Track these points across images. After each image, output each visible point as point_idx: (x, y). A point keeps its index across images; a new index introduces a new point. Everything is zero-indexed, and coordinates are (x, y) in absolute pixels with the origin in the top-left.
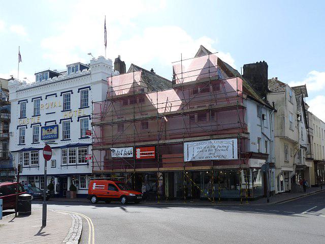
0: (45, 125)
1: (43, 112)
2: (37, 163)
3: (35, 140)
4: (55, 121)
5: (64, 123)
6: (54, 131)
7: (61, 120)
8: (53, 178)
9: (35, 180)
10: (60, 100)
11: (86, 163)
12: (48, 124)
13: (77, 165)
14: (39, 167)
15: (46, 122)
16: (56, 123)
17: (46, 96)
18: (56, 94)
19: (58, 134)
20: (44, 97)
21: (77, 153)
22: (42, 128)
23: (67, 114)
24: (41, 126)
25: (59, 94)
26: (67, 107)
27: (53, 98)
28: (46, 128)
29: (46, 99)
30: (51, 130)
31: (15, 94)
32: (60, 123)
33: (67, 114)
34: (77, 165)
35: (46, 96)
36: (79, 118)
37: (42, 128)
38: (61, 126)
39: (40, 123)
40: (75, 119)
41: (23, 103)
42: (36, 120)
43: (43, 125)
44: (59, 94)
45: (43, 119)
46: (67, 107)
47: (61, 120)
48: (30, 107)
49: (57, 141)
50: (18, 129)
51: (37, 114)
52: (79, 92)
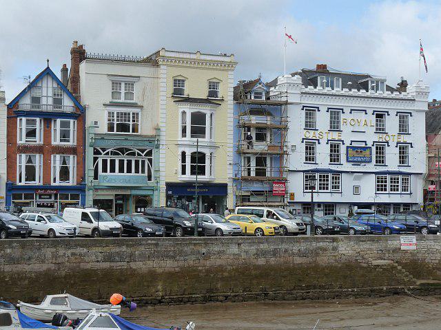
4: (365, 142)
5: (377, 148)
9: (316, 208)
11: (409, 192)
15: (352, 141)
16: (366, 145)
18: (365, 111)
20: (347, 110)
21: (400, 180)
22: (348, 147)
25: (370, 112)
26: (380, 130)
29: (351, 113)
31: (299, 96)
32: (373, 145)
33: (383, 138)
36: (397, 143)
37: (348, 147)
38: (374, 149)
39: (343, 141)
40: (393, 144)
42: (335, 135)
44: (370, 112)
45: (347, 136)
46: (380, 130)
47: (374, 142)
48: (322, 120)
49: (368, 165)
50: (303, 142)
51: (335, 126)
52: (397, 115)
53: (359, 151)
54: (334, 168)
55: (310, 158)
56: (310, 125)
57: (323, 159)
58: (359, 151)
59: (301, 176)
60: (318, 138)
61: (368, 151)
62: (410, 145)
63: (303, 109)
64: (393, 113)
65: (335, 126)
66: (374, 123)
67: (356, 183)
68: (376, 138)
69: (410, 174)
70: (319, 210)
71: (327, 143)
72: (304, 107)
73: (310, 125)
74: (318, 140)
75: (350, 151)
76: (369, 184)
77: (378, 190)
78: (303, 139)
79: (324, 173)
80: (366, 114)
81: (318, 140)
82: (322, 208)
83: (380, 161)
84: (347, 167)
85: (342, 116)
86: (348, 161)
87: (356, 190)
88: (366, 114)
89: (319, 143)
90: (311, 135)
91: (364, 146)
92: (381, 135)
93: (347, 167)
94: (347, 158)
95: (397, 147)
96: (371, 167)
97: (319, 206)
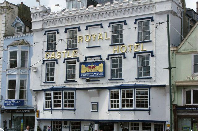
0: (85, 60)
1: (82, 46)
2: (73, 106)
3: (70, 78)
4: (100, 56)
5: (113, 61)
6: (100, 68)
7: (109, 55)
8: (91, 124)
9: (63, 125)
10: (107, 33)
12: (89, 60)
13: (52, 110)
14: (75, 110)
15: (86, 58)
16: (101, 59)
17: (87, 27)
18: (101, 25)
19: (104, 72)
20: (83, 28)
22: (81, 64)
23: (119, 50)
24: (78, 61)
25: (105, 25)
26: (117, 39)
27: (98, 30)
28: (86, 64)
29: (86, 29)
30: (94, 67)
32: (108, 59)
33: (119, 50)
34: (52, 110)
35: (87, 27)
37: (81, 64)
38: (108, 63)
39: (78, 58)
40: (130, 55)
41: (51, 36)
42: (71, 54)
43: (82, 60)
45: (83, 53)
46: (117, 39)
47: (109, 55)
49: (102, 81)
51: (72, 45)
53: (92, 66)
54: (68, 85)
55: (50, 77)
56: (51, 47)
57: (60, 80)
58: (92, 66)
59: (42, 96)
60: (56, 59)
61: (101, 65)
62: (150, 54)
63: (45, 34)
64: (130, 22)
65: (72, 45)
66: (110, 37)
67: (94, 100)
68: (111, 51)
69: (150, 87)
70: (66, 127)
71: (64, 62)
72: (46, 32)
73: (51, 47)
74: (56, 60)
75: (83, 66)
76: (105, 100)
77: (112, 107)
78: (44, 61)
79: (57, 92)
80: (102, 27)
81: (56, 60)
82: (68, 125)
83: (117, 72)
84: (81, 83)
85: (79, 34)
86: (80, 77)
87: (95, 107)
88: (102, 27)
89: (57, 63)
90: (51, 56)
91: (99, 60)
92: (117, 48)
93: (81, 83)
94: (80, 74)
95: (134, 57)
96: (105, 83)
97: (66, 123)
